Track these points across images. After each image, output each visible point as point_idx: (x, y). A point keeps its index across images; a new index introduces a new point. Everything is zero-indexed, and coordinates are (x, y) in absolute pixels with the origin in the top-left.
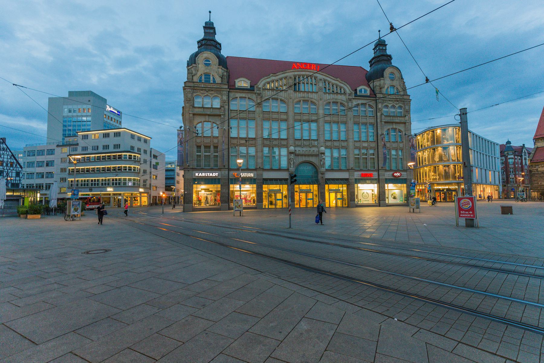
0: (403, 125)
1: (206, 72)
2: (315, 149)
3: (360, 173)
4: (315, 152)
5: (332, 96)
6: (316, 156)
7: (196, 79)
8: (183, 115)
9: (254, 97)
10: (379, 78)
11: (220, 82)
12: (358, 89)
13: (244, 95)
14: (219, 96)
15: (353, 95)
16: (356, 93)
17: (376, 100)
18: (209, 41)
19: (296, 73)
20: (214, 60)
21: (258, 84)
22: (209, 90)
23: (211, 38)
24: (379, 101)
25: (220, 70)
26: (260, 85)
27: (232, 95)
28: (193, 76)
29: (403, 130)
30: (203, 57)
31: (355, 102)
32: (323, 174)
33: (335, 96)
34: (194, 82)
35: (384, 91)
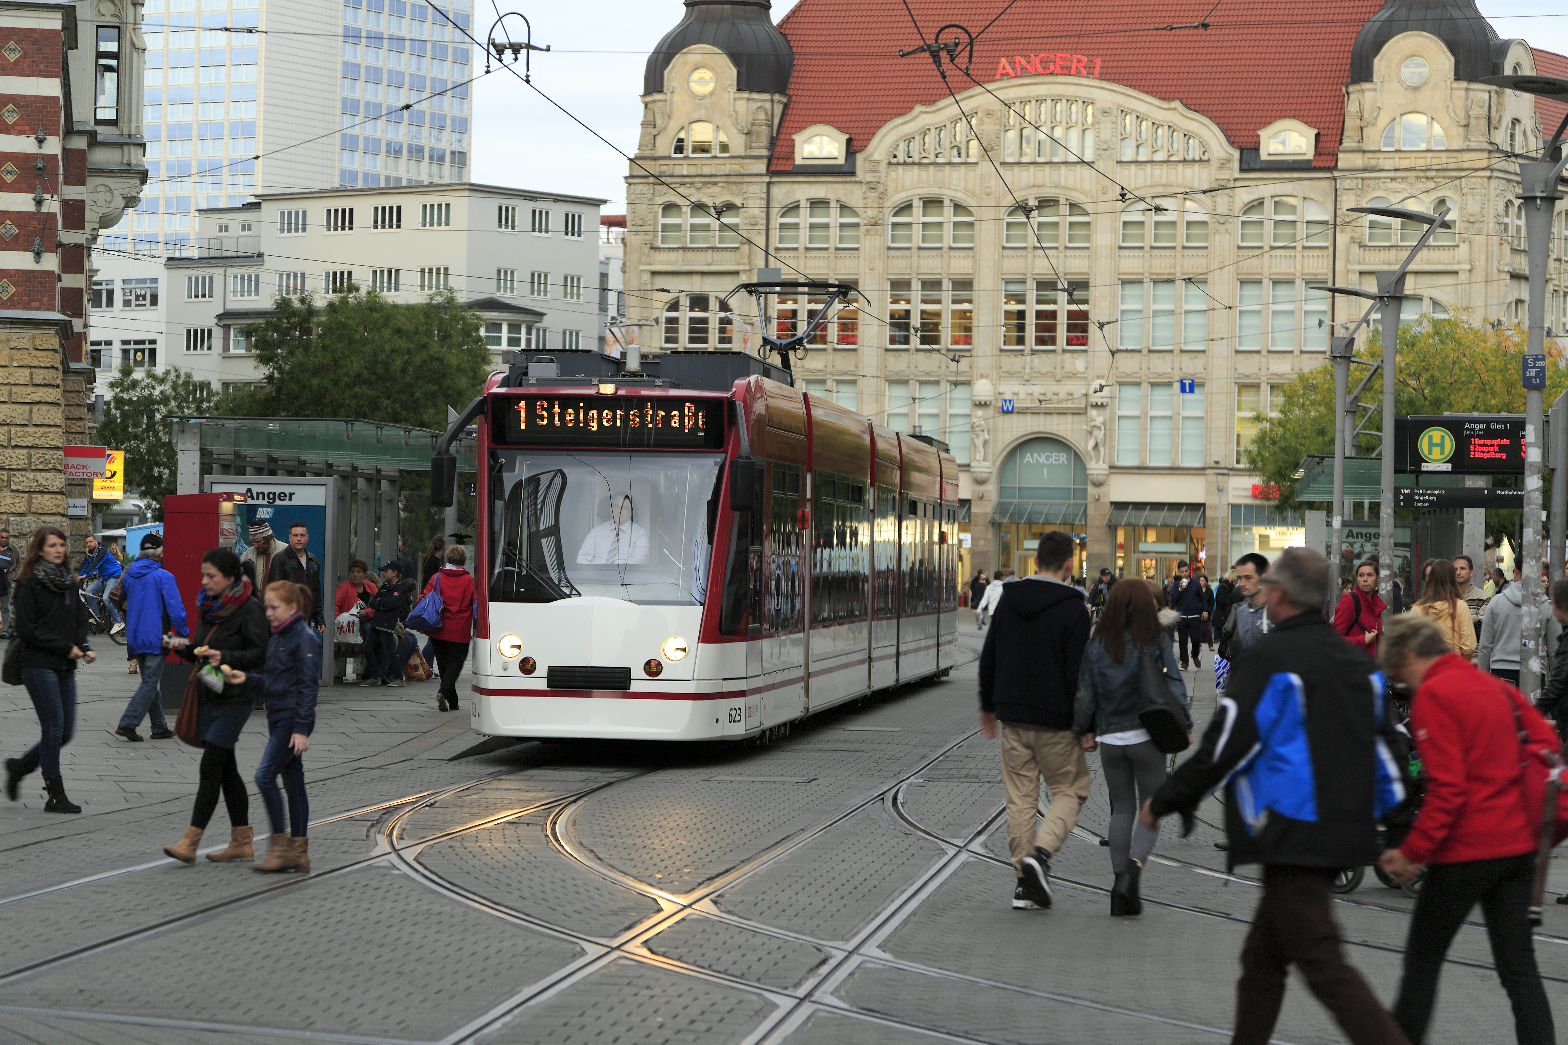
1: (695, 117)
11: (741, 152)
13: (819, 191)
15: (1236, 165)
17: (1335, 179)
22: (705, 183)
24: (1347, 184)
25: (742, 106)
32: (1098, 485)
33: (1160, 173)
34: (655, 159)
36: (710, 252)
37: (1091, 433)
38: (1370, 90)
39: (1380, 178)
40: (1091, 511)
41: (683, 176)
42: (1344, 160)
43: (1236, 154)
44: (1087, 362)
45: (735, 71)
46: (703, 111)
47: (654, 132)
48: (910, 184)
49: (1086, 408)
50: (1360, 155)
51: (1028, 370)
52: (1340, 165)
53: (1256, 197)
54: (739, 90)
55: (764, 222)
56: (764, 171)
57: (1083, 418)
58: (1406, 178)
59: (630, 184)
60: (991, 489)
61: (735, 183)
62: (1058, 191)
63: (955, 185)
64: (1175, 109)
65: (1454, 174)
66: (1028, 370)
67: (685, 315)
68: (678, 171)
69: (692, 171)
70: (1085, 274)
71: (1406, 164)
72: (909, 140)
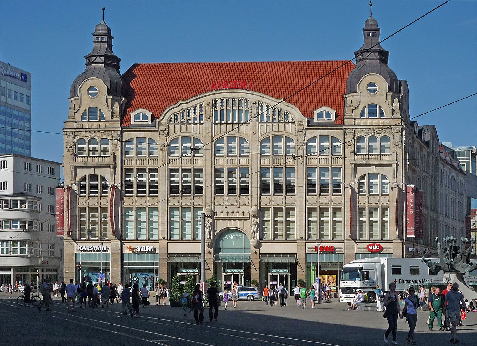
2: (246, 210)
12: (316, 113)
13: (141, 134)
19: (217, 96)
24: (347, 131)
27: (126, 136)
31: (309, 134)
42: (346, 122)
43: (306, 119)
46: (94, 103)
48: (176, 131)
52: (345, 123)
63: (194, 131)
69: (90, 126)
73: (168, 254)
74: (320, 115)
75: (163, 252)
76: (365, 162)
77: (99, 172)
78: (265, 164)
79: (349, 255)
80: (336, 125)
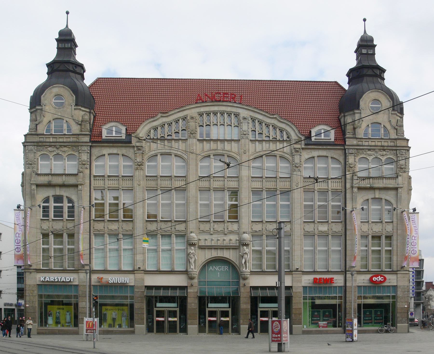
0: (393, 193)
2: (234, 238)
3: (311, 277)
4: (234, 241)
5: (265, 146)
6: (235, 248)
7: (41, 129)
8: (22, 186)
9: (130, 152)
10: (352, 110)
11: (78, 132)
14: (76, 154)
16: (309, 137)
17: (345, 149)
18: (64, 66)
19: (202, 110)
20: (69, 98)
21: (138, 131)
22: (61, 146)
23: (66, 59)
24: (351, 151)
26: (142, 131)
28: (37, 125)
29: (393, 201)
30: (53, 94)
31: (306, 155)
34: (38, 135)
35: (360, 133)
36: (64, 177)
37: (243, 257)
38: (358, 113)
39: (363, 149)
40: (242, 290)
41: (50, 142)
44: (239, 226)
45: (75, 97)
47: (37, 122)
49: (239, 246)
50: (355, 140)
51: (212, 230)
53: (311, 156)
54: (76, 105)
55: (89, 163)
56: (89, 141)
57: (237, 250)
58: (375, 149)
59: (25, 146)
60: (196, 281)
61: (75, 146)
62: (224, 152)
64: (275, 118)
65: (394, 148)
66: (212, 230)
67: (52, 204)
68: (48, 140)
69: (55, 140)
70: (237, 188)
71: (373, 144)
72: (156, 129)
73: (146, 286)
74: (318, 134)
75: (139, 285)
76: (369, 186)
77: (64, 193)
78: (257, 187)
79: (351, 287)
80: (336, 145)
